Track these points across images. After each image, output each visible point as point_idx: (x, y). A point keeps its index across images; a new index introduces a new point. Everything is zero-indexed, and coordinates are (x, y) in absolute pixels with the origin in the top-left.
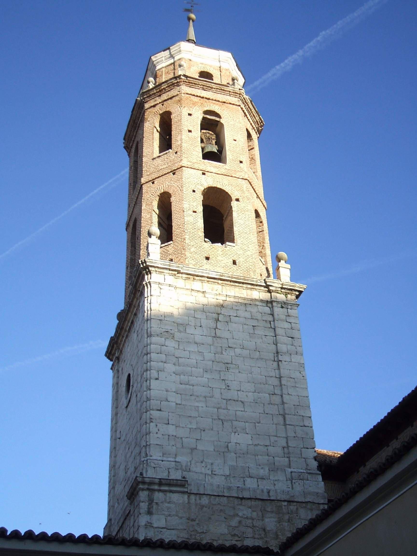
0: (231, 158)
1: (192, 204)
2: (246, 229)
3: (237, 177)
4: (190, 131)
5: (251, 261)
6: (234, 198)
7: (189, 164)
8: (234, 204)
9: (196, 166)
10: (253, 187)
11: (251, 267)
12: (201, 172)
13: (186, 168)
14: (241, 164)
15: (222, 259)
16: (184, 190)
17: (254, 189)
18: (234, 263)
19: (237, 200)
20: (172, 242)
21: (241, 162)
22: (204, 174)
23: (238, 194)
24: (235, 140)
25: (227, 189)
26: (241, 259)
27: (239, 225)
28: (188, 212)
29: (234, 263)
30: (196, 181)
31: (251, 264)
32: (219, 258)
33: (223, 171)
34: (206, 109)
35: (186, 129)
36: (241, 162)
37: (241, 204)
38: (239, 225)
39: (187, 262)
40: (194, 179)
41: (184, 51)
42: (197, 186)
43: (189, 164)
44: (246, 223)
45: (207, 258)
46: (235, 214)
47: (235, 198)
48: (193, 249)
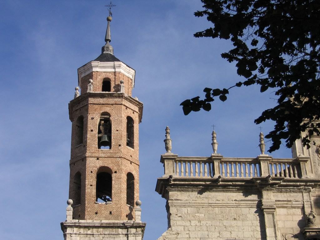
0: (114, 144)
1: (90, 181)
2: (118, 191)
3: (116, 157)
4: (92, 131)
5: (119, 211)
6: (113, 171)
7: (90, 154)
8: (114, 175)
9: (94, 155)
10: (127, 159)
11: (119, 214)
12: (96, 158)
13: (88, 158)
14: (120, 147)
15: (104, 212)
16: (86, 172)
17: (128, 160)
18: (111, 213)
19: (116, 172)
20: (80, 205)
21: (120, 145)
22: (98, 159)
23: (116, 168)
24: (117, 131)
25: (110, 166)
26: (114, 210)
27: (115, 189)
28: (88, 186)
29: (111, 213)
30: (93, 165)
31: (119, 212)
32: (103, 212)
33: (109, 155)
34: (102, 112)
35: (90, 129)
36: (120, 145)
37: (118, 174)
38: (115, 189)
39: (86, 218)
40: (92, 164)
41: (94, 66)
42: (94, 168)
43: (90, 154)
44: (119, 187)
45: (96, 213)
46: (113, 182)
47: (114, 171)
48: (89, 209)
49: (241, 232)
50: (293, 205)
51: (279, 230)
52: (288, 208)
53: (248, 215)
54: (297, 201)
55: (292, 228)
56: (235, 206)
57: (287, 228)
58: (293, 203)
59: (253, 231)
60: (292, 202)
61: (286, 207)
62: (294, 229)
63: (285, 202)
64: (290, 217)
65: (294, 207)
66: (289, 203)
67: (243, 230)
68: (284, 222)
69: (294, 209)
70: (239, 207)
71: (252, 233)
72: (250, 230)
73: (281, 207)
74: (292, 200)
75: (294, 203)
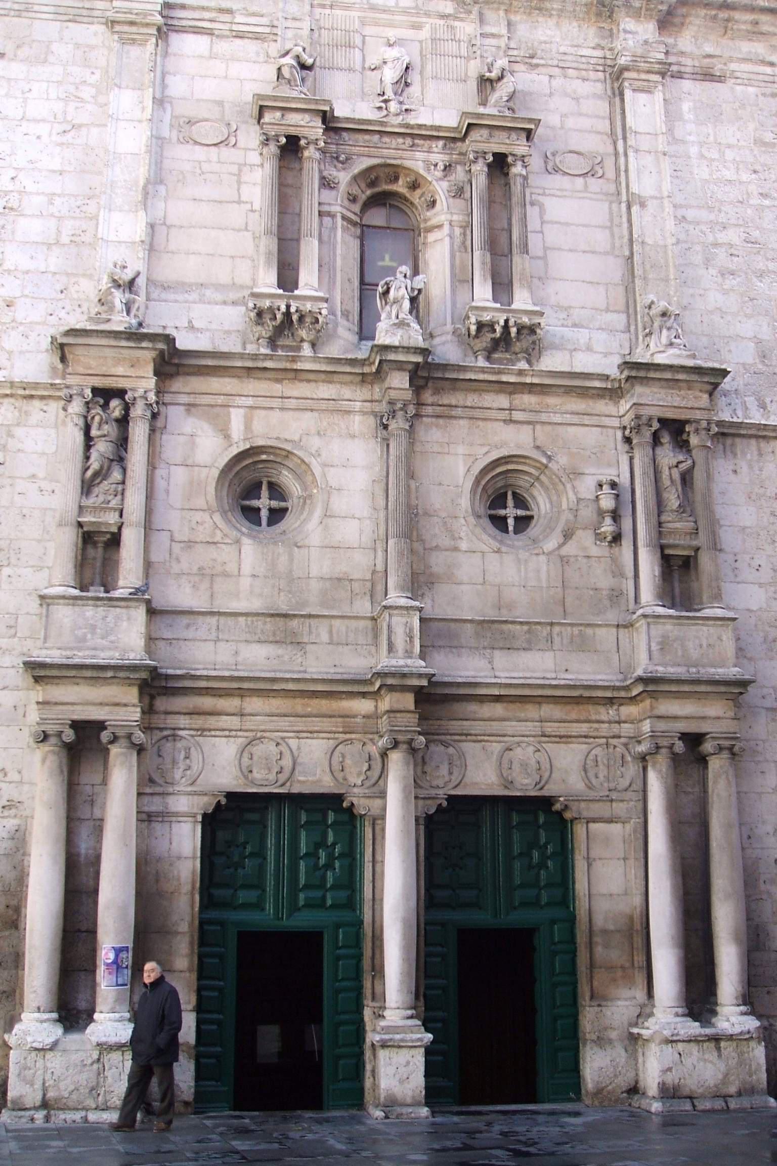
49: (16, 98)
50: (235, 27)
51: (168, 106)
52: (218, 36)
53: (55, 47)
54: (254, 14)
55: (220, 103)
56: (12, 13)
57: (198, 100)
58: (236, 20)
59: (66, 100)
60: (234, 17)
61: (209, 32)
62: (226, 105)
63: (207, 15)
64: (219, 67)
65: (241, 34)
66: (226, 18)
67: (27, 95)
68: (193, 79)
69: (238, 41)
70: (24, 14)
71: (58, 107)
72: (53, 95)
73: (191, 29)
74: (234, 8)
75: (239, 19)
